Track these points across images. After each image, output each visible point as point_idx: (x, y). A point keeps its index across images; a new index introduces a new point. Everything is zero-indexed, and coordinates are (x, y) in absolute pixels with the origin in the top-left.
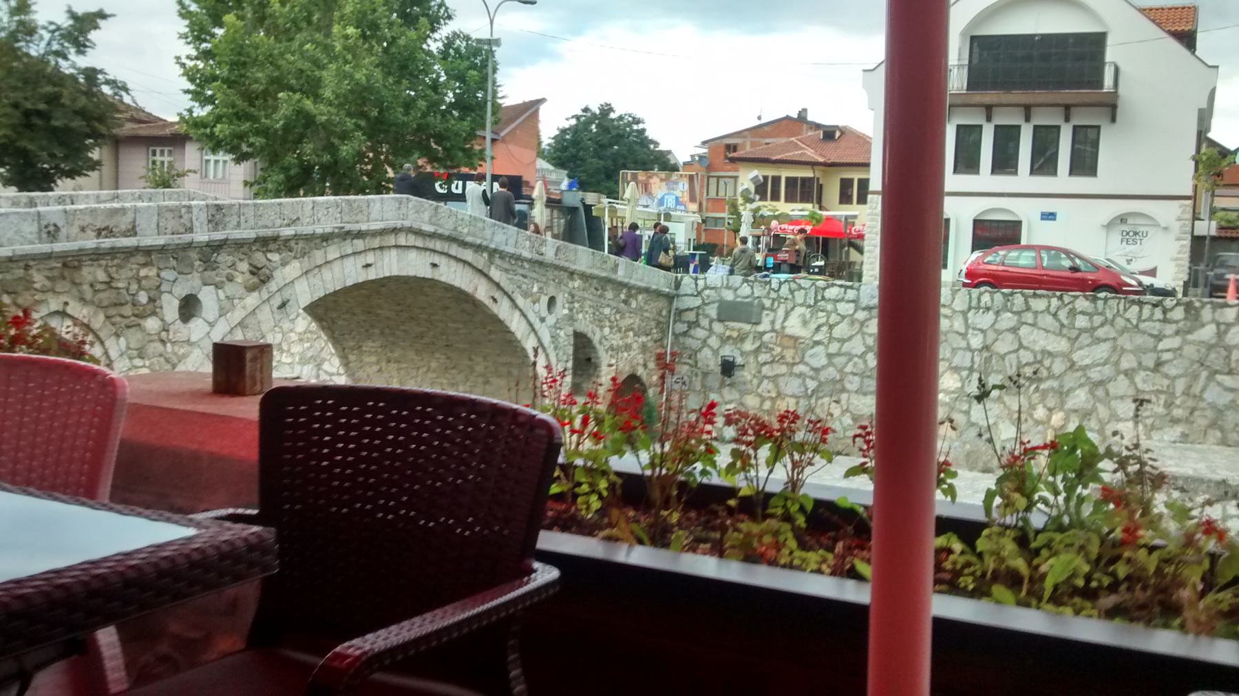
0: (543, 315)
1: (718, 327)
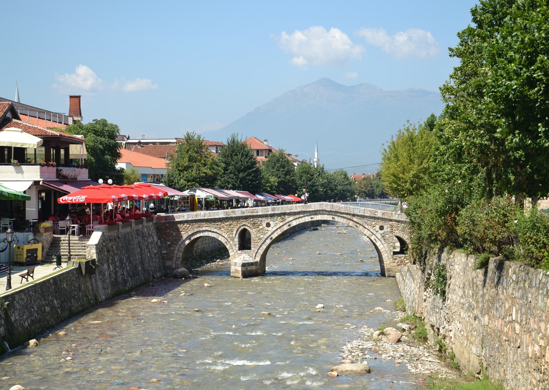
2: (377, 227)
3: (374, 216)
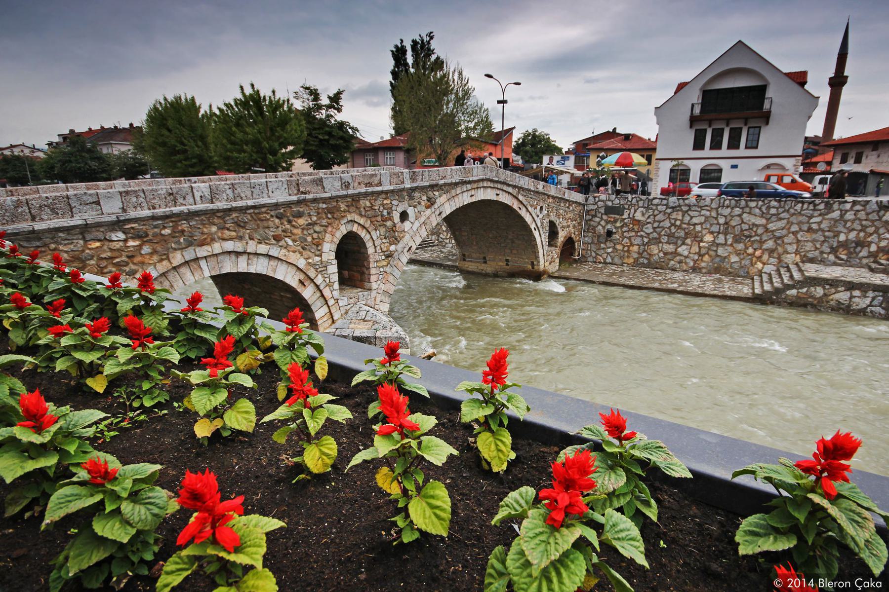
1: (605, 217)
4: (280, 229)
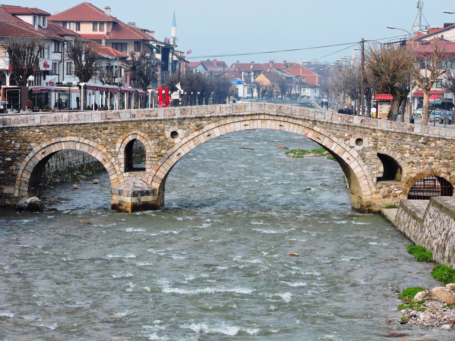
0: (352, 145)
2: (352, 141)
3: (347, 123)
4: (96, 134)
